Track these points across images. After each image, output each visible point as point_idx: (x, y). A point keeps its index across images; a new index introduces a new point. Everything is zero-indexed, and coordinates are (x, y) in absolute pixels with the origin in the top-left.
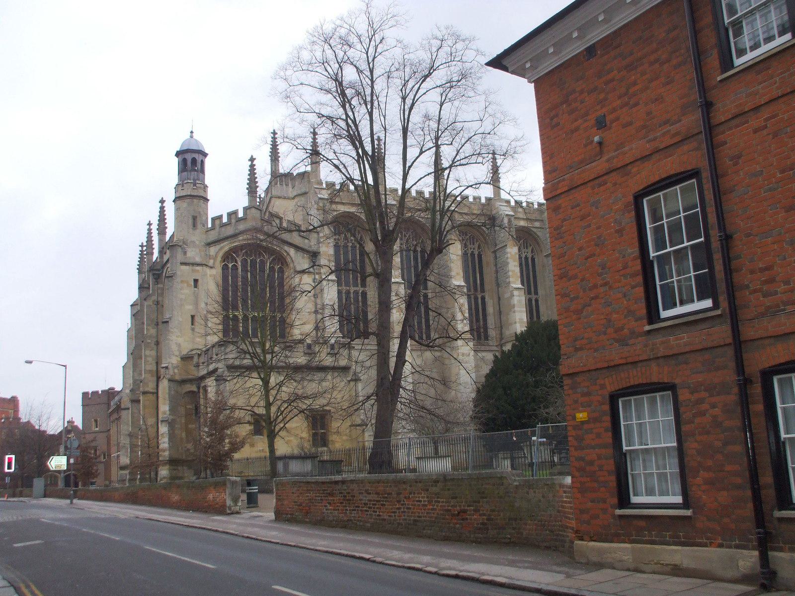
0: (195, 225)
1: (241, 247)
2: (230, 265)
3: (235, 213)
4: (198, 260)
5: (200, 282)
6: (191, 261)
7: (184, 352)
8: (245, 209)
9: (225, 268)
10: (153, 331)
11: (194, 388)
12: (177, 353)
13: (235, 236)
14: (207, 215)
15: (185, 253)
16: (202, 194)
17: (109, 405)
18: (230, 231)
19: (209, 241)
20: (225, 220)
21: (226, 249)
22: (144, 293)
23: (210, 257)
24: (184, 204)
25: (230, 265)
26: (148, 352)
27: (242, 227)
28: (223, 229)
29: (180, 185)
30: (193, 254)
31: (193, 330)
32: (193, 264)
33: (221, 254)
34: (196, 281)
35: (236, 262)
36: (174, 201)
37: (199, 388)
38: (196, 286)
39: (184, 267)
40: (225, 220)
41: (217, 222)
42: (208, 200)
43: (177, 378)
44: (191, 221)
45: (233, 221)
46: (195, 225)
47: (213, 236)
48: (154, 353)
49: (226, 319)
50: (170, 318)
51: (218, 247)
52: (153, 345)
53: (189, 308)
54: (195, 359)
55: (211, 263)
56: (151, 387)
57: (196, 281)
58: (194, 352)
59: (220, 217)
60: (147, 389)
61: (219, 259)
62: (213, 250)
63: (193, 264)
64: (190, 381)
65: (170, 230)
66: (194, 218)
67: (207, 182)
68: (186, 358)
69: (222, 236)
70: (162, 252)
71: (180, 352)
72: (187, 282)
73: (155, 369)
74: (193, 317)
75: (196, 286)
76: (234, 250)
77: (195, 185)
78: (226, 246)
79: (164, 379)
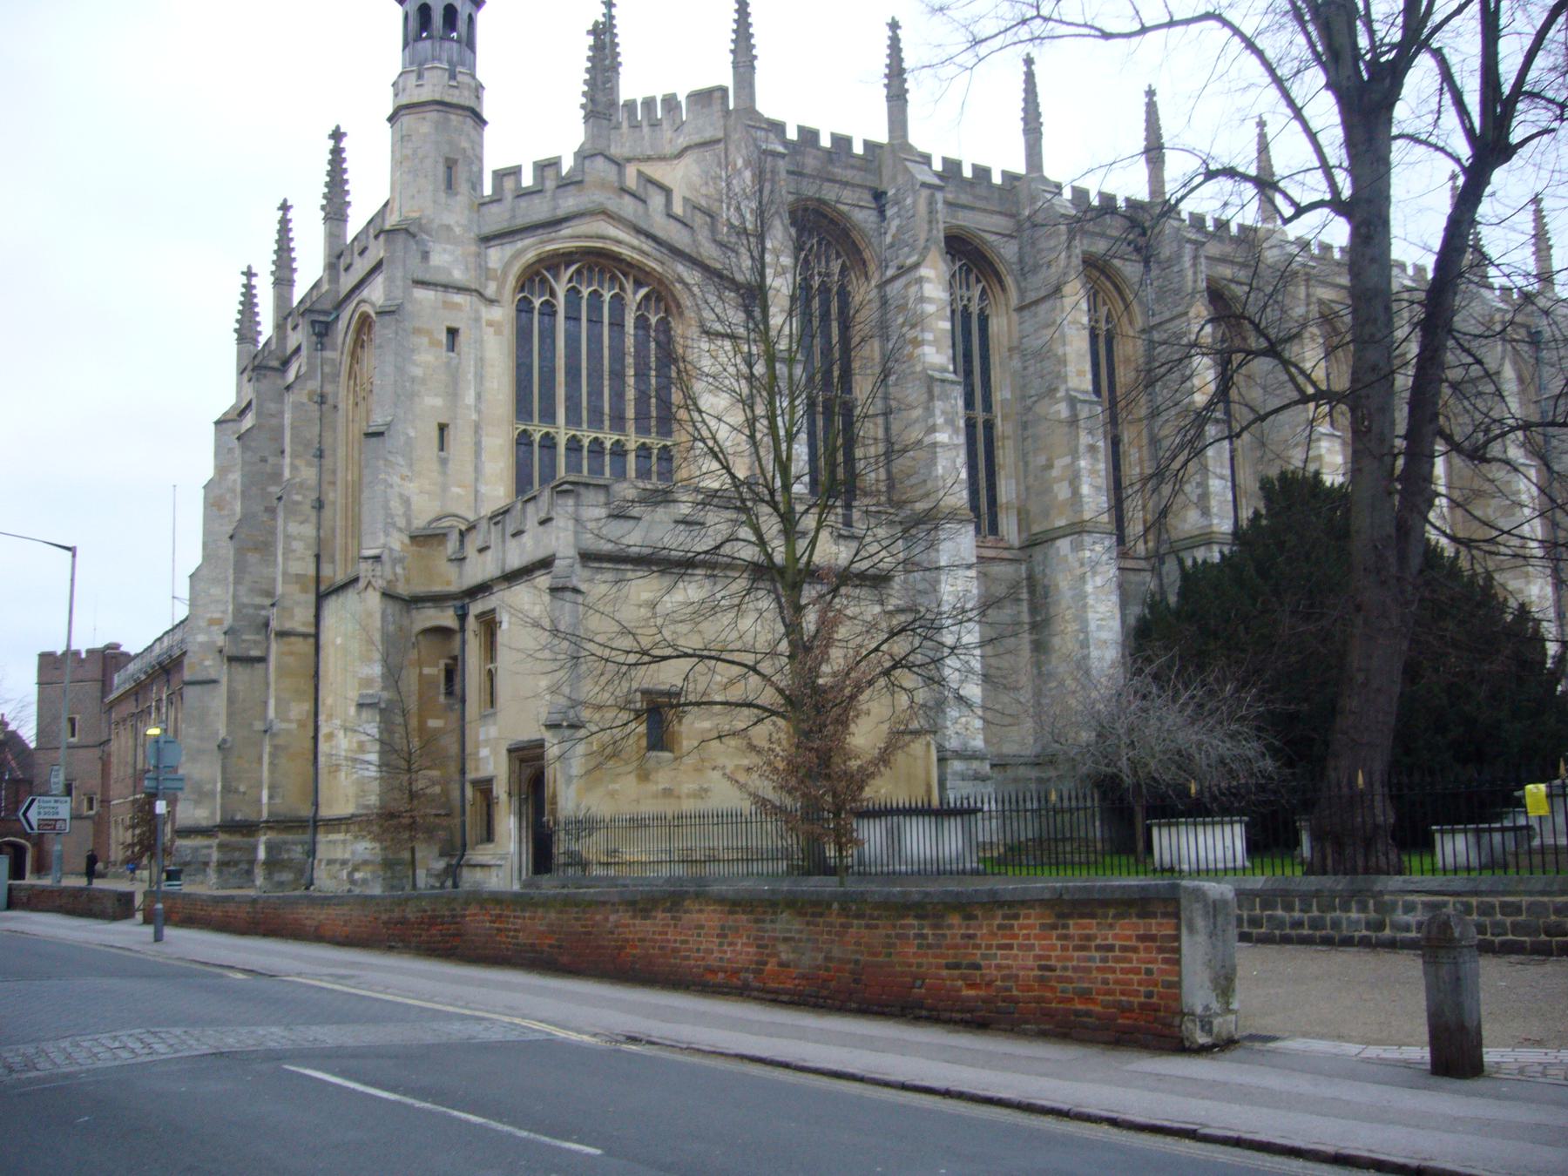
0: (450, 185)
1: (567, 258)
2: (537, 303)
3: (554, 163)
4: (458, 275)
5: (462, 338)
6: (442, 278)
7: (419, 522)
8: (582, 156)
9: (524, 307)
10: (309, 474)
11: (447, 618)
12: (401, 523)
13: (555, 223)
14: (480, 160)
15: (425, 256)
16: (465, 99)
17: (105, 684)
18: (539, 210)
19: (490, 228)
20: (527, 180)
21: (530, 256)
22: (271, 382)
23: (485, 272)
24: (423, 125)
25: (537, 303)
26: (293, 528)
27: (569, 203)
28: (523, 203)
29: (415, 66)
30: (447, 260)
31: (444, 462)
32: (446, 287)
33: (516, 269)
34: (452, 332)
35: (553, 294)
36: (391, 119)
37: (462, 617)
38: (452, 347)
39: (420, 294)
40: (527, 180)
41: (509, 184)
42: (484, 123)
43: (402, 589)
44: (441, 169)
45: (550, 184)
46: (450, 185)
47: (497, 218)
48: (309, 530)
49: (523, 440)
50: (388, 425)
51: (509, 250)
52: (307, 508)
53: (432, 403)
54: (452, 545)
55: (491, 290)
56: (300, 619)
57: (452, 332)
58: (446, 523)
59: (516, 172)
60: (288, 625)
61: (511, 281)
62: (496, 256)
63: (446, 287)
64: (438, 600)
65: (365, 201)
66: (450, 165)
67: (481, 74)
68: (427, 538)
69: (520, 222)
70: (336, 260)
71: (409, 522)
72: (429, 333)
73: (311, 571)
74: (442, 428)
75: (452, 347)
76: (555, 262)
77: (453, 76)
78: (530, 249)
79: (370, 590)
